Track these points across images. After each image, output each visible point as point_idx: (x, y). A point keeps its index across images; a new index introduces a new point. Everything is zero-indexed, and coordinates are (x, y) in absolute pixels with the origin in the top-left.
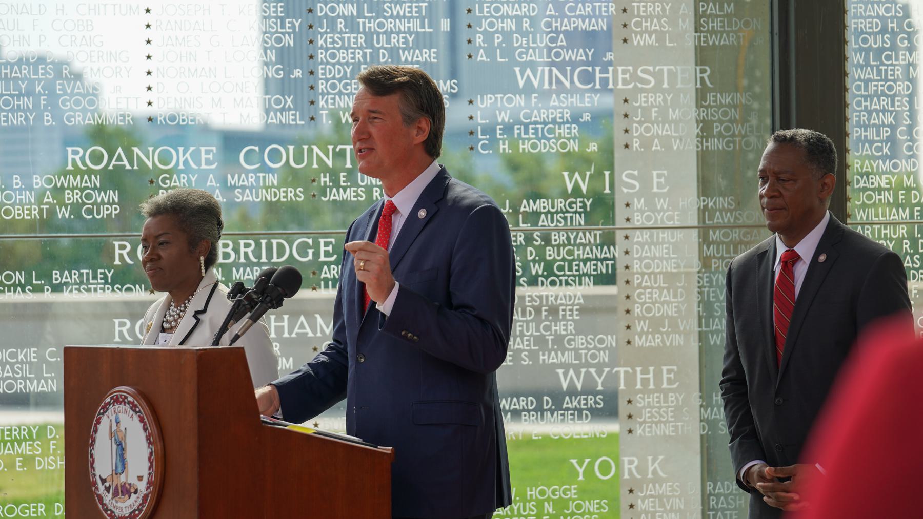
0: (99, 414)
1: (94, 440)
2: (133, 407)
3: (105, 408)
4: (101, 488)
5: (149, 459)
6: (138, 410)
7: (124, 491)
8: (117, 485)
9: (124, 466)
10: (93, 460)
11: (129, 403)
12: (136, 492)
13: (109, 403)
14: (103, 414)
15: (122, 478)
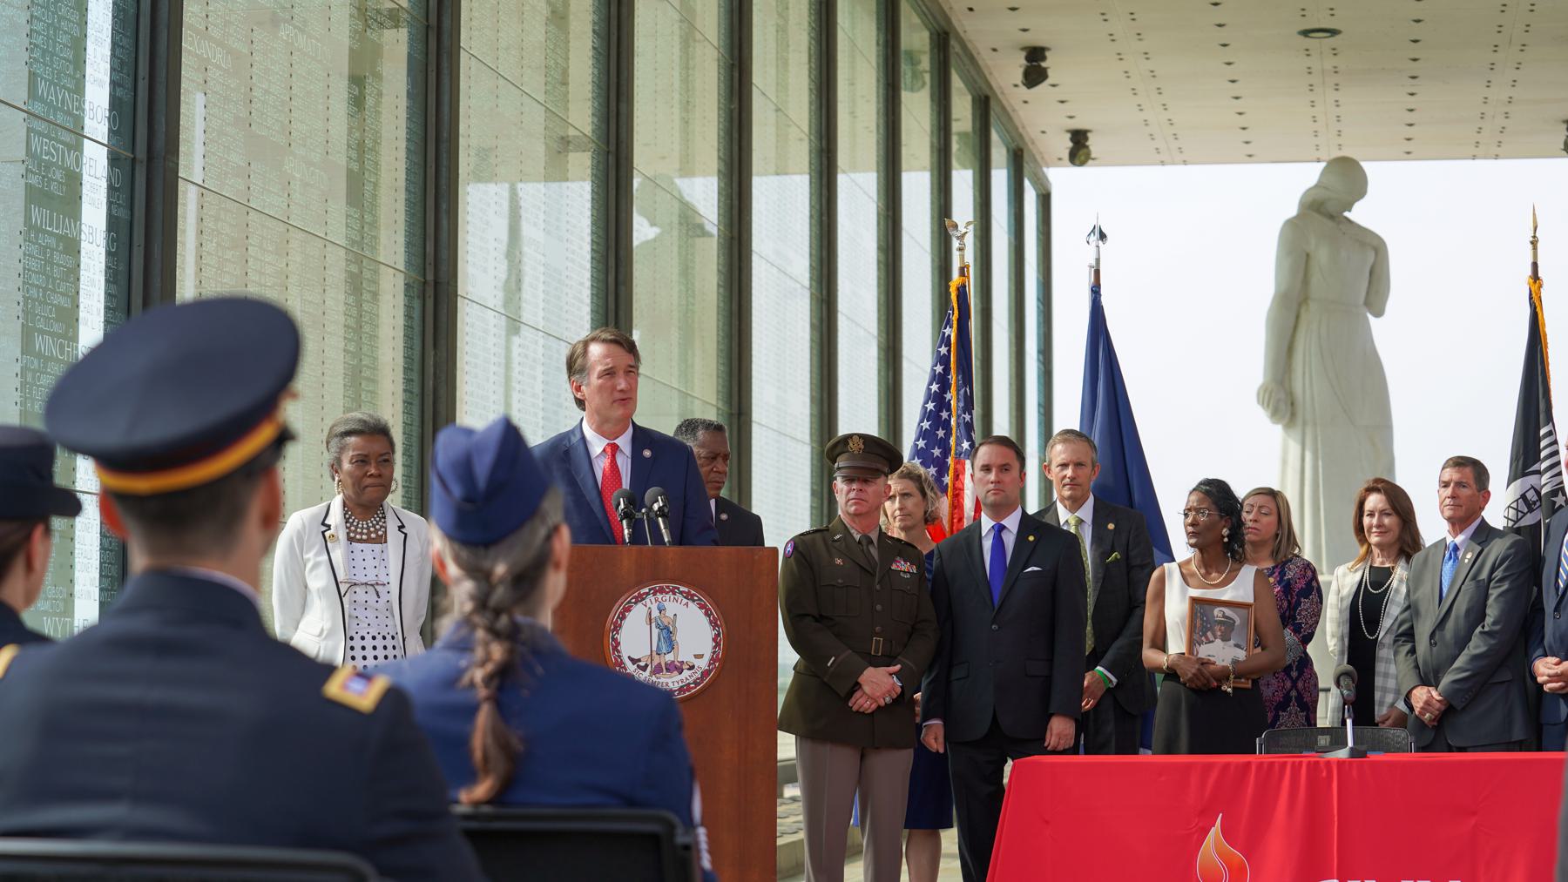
0: (629, 602)
1: (617, 628)
2: (689, 597)
3: (640, 598)
4: (631, 668)
5: (714, 640)
6: (696, 598)
7: (672, 668)
8: (660, 664)
9: (672, 646)
10: (618, 644)
11: (681, 593)
12: (691, 668)
13: (648, 594)
14: (636, 603)
15: (669, 657)
